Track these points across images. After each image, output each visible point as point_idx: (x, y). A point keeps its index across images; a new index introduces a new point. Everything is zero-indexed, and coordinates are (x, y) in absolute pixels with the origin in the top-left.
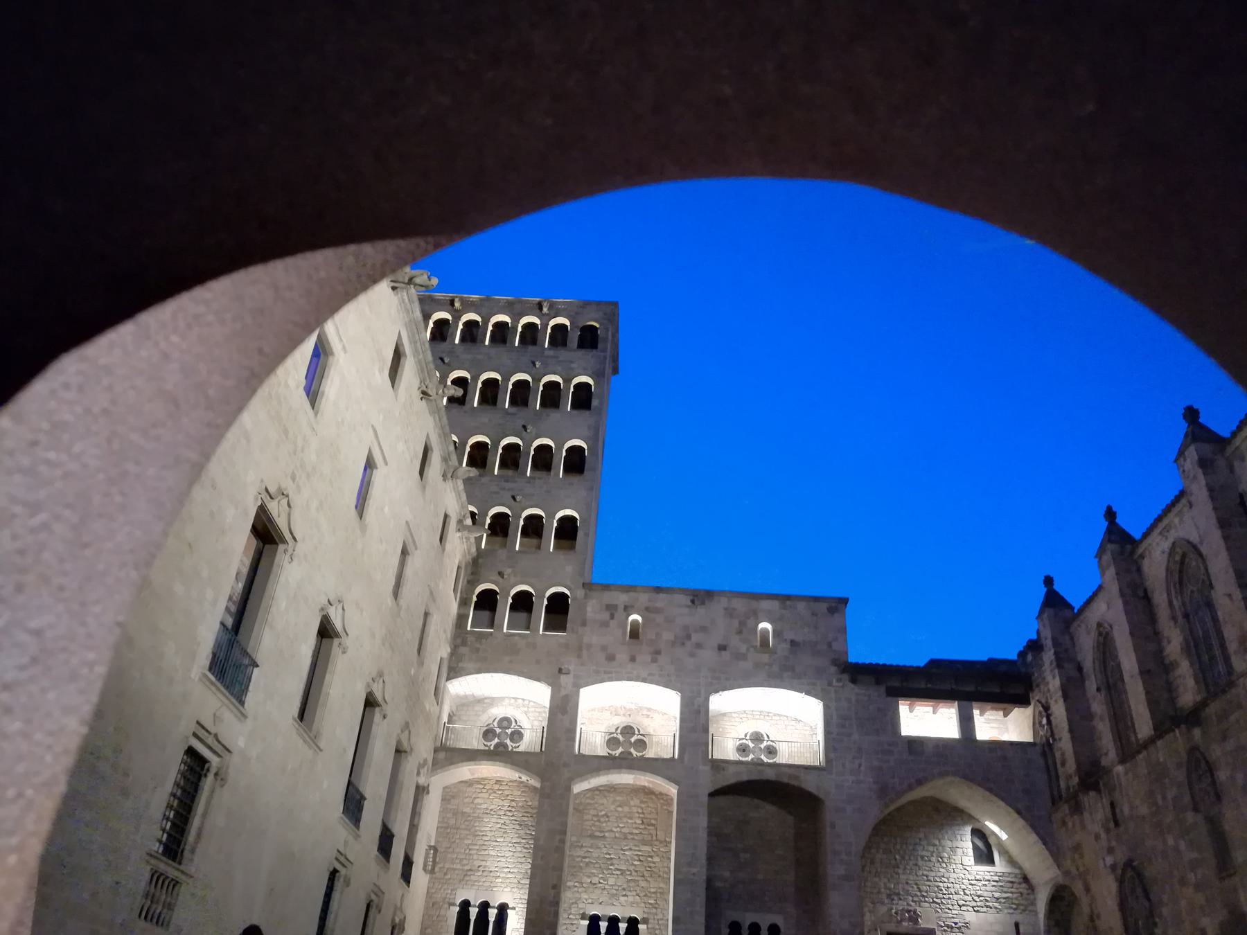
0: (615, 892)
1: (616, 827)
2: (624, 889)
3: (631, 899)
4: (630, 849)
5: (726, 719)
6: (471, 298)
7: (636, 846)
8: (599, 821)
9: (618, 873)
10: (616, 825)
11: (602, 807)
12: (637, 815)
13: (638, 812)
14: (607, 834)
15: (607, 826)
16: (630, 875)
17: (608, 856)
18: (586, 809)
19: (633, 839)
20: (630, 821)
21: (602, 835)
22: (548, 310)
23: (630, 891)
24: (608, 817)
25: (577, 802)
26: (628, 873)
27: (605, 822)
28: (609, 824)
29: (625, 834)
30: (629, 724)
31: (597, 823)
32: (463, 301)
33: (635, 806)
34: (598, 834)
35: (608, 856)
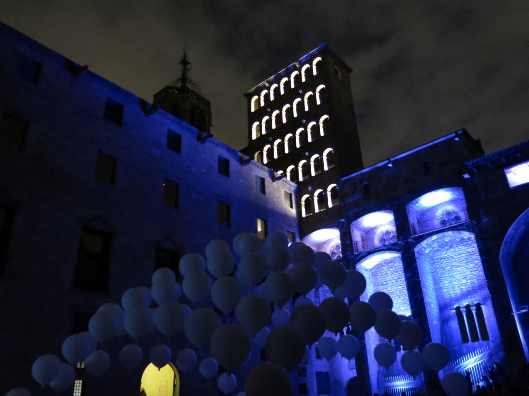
0: (398, 306)
1: (391, 278)
2: (402, 304)
3: (406, 307)
4: (400, 286)
5: (430, 212)
6: (271, 79)
7: (402, 283)
8: (384, 277)
9: (398, 297)
10: (391, 277)
11: (383, 271)
12: (399, 270)
13: (399, 269)
14: (389, 282)
15: (388, 278)
16: (403, 297)
17: (391, 291)
18: (377, 274)
19: (400, 281)
20: (397, 273)
21: (386, 283)
22: (299, 65)
23: (404, 304)
24: (387, 274)
25: (373, 272)
26: (402, 296)
27: (386, 277)
28: (389, 277)
29: (396, 280)
30: (388, 230)
31: (383, 279)
32: (268, 82)
33: (397, 266)
34: (384, 283)
35: (391, 291)
